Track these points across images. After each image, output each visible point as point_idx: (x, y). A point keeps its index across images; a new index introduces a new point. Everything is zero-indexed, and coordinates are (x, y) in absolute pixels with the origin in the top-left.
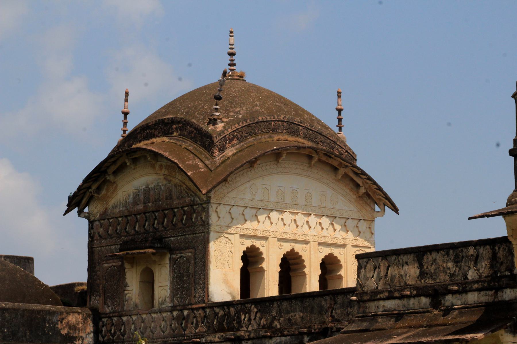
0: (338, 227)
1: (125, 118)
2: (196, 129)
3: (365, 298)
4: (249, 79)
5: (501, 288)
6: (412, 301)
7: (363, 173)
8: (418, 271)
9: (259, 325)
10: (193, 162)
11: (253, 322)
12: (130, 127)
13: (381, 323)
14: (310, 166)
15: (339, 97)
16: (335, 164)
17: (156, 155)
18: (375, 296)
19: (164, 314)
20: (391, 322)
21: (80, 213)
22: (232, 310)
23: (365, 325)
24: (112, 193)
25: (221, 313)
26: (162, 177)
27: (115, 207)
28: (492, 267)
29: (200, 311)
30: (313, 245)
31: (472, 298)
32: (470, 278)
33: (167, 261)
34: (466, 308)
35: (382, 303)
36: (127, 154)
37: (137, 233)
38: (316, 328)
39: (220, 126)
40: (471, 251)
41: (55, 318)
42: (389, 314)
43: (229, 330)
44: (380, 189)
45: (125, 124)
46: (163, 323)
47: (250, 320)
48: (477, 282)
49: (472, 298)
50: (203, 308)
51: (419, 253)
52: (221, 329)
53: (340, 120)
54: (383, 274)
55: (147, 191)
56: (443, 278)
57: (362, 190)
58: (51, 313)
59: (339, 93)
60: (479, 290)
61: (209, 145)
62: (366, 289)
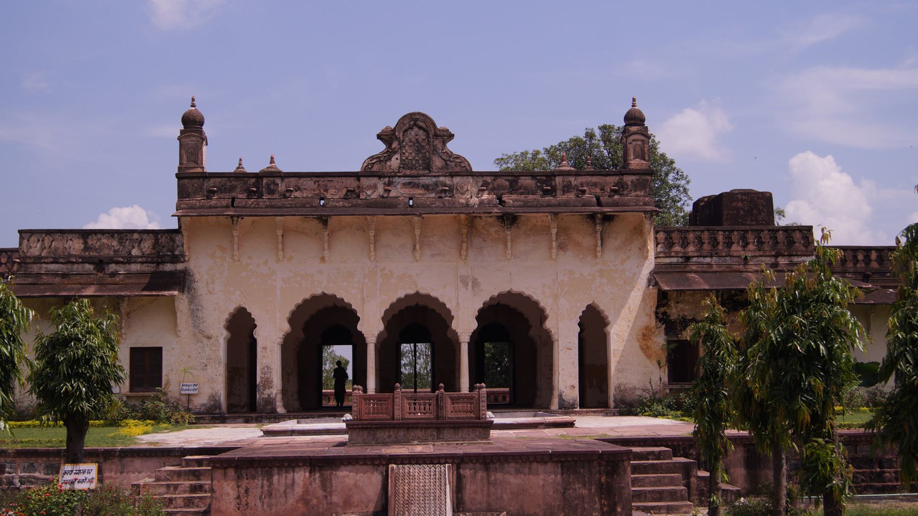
3: (28, 261)
5: (163, 263)
6: (76, 266)
8: (82, 246)
13: (45, 279)
18: (38, 260)
20: (57, 280)
23: (30, 280)
28: (154, 248)
31: (135, 267)
32: (133, 253)
34: (129, 274)
35: (44, 266)
40: (136, 236)
48: (141, 257)
49: (135, 267)
51: (85, 234)
56: (106, 252)
60: (142, 263)
62: (28, 254)
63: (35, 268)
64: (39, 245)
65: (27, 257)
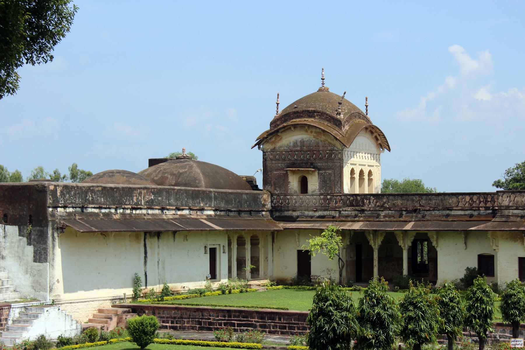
0: (372, 158)
1: (278, 106)
2: (330, 116)
3: (502, 208)
4: (330, 90)
7: (384, 135)
9: (376, 205)
10: (334, 132)
11: (371, 203)
12: (280, 111)
13: (512, 219)
14: (366, 132)
15: (366, 100)
16: (374, 131)
17: (309, 126)
18: (508, 208)
19: (315, 197)
20: (519, 219)
21: (259, 148)
22: (359, 198)
23: (504, 219)
24: (279, 141)
25: (352, 198)
26: (312, 136)
27: (281, 147)
29: (338, 197)
30: (367, 166)
33: (316, 173)
35: (511, 211)
36: (283, 123)
37: (296, 160)
38: (410, 208)
39: (342, 116)
41: (261, 196)
42: (517, 216)
43: (357, 206)
44: (387, 142)
45: (278, 108)
46: (314, 201)
47: (370, 202)
50: (340, 196)
52: (351, 205)
53: (367, 110)
54: (512, 199)
55: (302, 142)
57: (379, 142)
58: (259, 194)
59: (366, 98)
61: (339, 124)
62: (502, 205)
63: (506, 212)
64: (508, 200)
65: (501, 206)
